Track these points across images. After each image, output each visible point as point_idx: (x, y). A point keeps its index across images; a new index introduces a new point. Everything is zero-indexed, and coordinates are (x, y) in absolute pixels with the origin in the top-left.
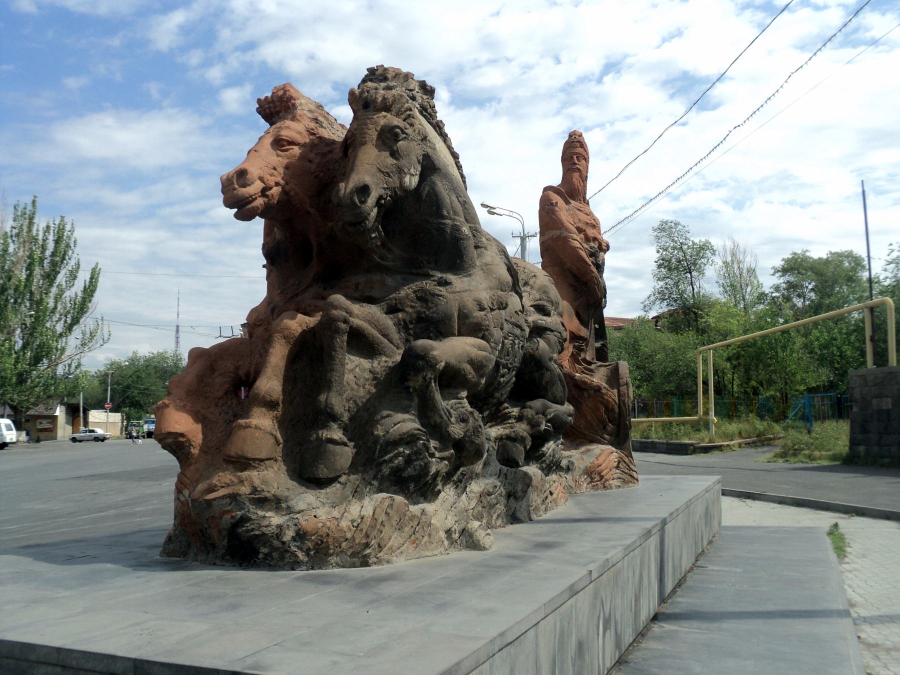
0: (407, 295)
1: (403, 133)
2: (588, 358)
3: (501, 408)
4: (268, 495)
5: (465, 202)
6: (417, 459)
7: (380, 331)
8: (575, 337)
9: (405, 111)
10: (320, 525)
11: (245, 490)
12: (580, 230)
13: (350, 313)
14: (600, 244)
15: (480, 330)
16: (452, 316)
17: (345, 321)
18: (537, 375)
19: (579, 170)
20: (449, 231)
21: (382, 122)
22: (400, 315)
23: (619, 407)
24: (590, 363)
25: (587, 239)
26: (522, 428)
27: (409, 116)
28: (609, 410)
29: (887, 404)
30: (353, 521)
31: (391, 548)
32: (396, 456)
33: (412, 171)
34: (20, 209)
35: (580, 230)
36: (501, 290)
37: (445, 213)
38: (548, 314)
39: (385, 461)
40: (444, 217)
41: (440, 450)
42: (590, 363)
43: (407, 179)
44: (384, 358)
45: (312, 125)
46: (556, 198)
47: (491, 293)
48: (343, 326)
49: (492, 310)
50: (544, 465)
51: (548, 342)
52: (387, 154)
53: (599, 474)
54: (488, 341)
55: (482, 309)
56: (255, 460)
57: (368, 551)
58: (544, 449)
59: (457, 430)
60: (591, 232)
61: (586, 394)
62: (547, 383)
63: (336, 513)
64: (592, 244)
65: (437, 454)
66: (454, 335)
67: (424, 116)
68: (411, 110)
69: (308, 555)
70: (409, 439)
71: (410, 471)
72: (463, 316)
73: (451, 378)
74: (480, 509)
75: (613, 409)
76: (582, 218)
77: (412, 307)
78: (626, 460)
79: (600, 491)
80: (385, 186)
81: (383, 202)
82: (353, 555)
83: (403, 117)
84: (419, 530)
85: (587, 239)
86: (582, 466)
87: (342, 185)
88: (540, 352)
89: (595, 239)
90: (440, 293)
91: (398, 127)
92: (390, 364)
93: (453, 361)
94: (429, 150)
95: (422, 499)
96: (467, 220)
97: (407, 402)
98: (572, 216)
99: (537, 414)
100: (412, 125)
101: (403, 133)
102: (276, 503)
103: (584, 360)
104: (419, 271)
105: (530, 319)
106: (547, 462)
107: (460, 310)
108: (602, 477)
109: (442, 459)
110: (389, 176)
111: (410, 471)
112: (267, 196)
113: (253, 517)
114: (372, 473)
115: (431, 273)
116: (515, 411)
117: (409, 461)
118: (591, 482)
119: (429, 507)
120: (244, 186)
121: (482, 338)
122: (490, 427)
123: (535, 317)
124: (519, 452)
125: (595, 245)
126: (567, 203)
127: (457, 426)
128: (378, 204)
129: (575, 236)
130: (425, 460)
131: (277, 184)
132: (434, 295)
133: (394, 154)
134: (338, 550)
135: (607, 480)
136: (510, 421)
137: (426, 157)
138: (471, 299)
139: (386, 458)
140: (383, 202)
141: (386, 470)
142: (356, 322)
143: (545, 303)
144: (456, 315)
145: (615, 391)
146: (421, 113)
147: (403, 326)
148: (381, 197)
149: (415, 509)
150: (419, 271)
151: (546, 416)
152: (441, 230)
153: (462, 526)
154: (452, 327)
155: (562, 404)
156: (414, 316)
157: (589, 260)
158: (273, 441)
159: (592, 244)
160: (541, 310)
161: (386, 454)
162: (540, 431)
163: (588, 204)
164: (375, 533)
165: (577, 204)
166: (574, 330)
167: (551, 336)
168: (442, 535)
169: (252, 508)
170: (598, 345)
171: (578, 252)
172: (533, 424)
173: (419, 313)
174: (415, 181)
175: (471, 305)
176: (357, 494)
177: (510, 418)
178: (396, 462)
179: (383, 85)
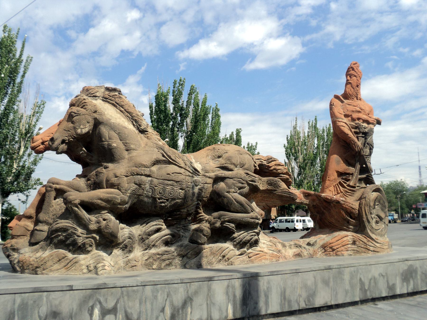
2: (351, 183)
3: (197, 216)
4: (15, 247)
5: (119, 133)
6: (71, 237)
8: (340, 174)
9: (83, 103)
11: (9, 245)
15: (115, 186)
16: (103, 180)
18: (220, 200)
19: (350, 83)
20: (106, 147)
23: (359, 210)
25: (353, 120)
26: (205, 226)
27: (84, 105)
28: (350, 213)
30: (36, 258)
31: (51, 270)
32: (60, 235)
33: (82, 127)
34: (311, 123)
35: (346, 116)
36: (136, 167)
37: (104, 140)
38: (231, 170)
39: (52, 238)
40: (103, 141)
41: (87, 234)
46: (337, 102)
47: (127, 169)
50: (235, 243)
51: (227, 184)
52: (70, 123)
53: (331, 248)
54: (120, 190)
55: (116, 177)
56: (15, 236)
57: (38, 269)
60: (355, 115)
61: (332, 205)
62: (227, 203)
63: (31, 255)
64: (357, 122)
65: (85, 236)
69: (20, 268)
70: (64, 230)
71: (68, 242)
72: (107, 181)
74: (151, 260)
75: (352, 213)
76: (349, 109)
77: (93, 178)
78: (365, 240)
79: (332, 257)
80: (67, 135)
81: (67, 141)
82: (33, 270)
85: (353, 120)
86: (321, 243)
88: (219, 189)
89: (359, 119)
91: (72, 112)
95: (82, 253)
96: (121, 140)
97: (68, 216)
98: (343, 109)
99: (214, 219)
100: (85, 109)
103: (349, 185)
105: (212, 175)
106: (237, 241)
108: (333, 250)
109: (87, 238)
110: (69, 131)
111: (68, 242)
113: (11, 254)
114: (49, 241)
115: (103, 164)
116: (207, 217)
117: (67, 238)
118: (325, 252)
119: (82, 256)
120: (33, 143)
121: (118, 189)
122: (193, 225)
126: (342, 102)
127: (95, 225)
129: (340, 120)
133: (73, 122)
134: (28, 268)
135: (338, 251)
136: (203, 222)
137: (95, 119)
139: (53, 236)
141: (55, 241)
143: (226, 165)
144: (105, 180)
145: (359, 201)
149: (70, 256)
151: (220, 220)
152: (103, 147)
153: (95, 265)
154: (103, 185)
156: (93, 182)
158: (25, 229)
159: (357, 122)
161: (53, 235)
162: (216, 227)
163: (360, 100)
165: (350, 101)
166: (340, 170)
167: (228, 181)
168: (84, 267)
169: (11, 251)
170: (364, 176)
171: (340, 129)
172: (212, 224)
173: (94, 180)
176: (43, 249)
177: (203, 221)
178: (59, 238)
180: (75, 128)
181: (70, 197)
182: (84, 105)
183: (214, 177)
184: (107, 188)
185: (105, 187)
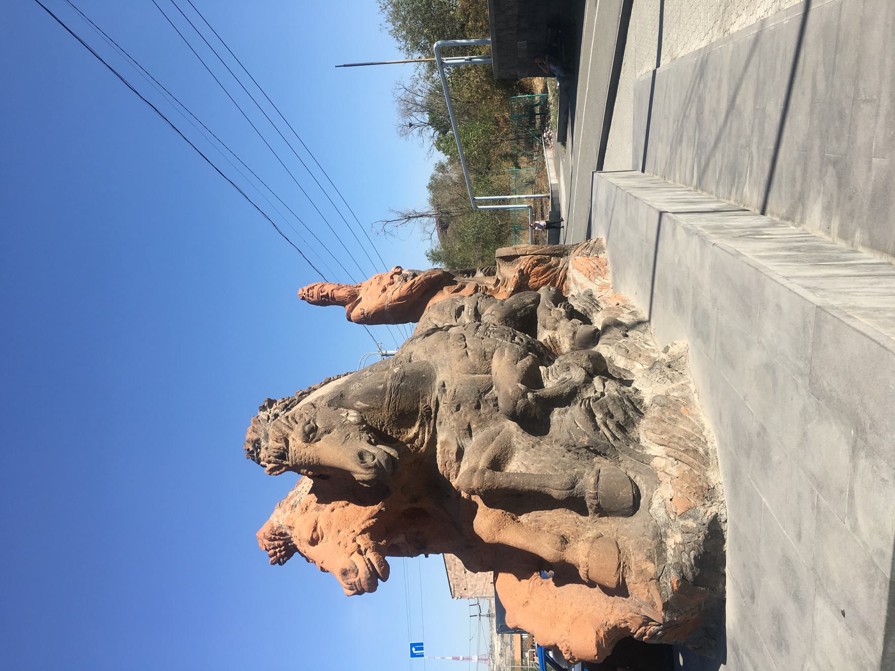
0: (455, 420)
1: (309, 423)
2: (494, 282)
7: (489, 444)
10: (679, 495)
12: (384, 290)
13: (473, 470)
14: (396, 273)
16: (474, 382)
17: (483, 472)
21: (299, 442)
22: (473, 426)
24: (498, 281)
29: (522, 45)
35: (384, 290)
40: (385, 388)
42: (498, 281)
43: (352, 419)
44: (514, 439)
45: (298, 509)
48: (487, 474)
49: (466, 346)
58: (579, 310)
59: (577, 375)
66: (490, 379)
67: (292, 407)
68: (287, 417)
73: (532, 379)
77: (465, 416)
81: (373, 440)
83: (293, 423)
84: (672, 406)
87: (357, 477)
89: (392, 277)
90: (452, 392)
91: (304, 427)
92: (520, 433)
93: (516, 377)
94: (323, 402)
101: (309, 423)
102: (659, 538)
104: (433, 410)
106: (591, 307)
107: (468, 373)
112: (366, 550)
123: (466, 317)
124: (583, 330)
125: (396, 277)
128: (375, 444)
130: (608, 400)
131: (354, 541)
132: (454, 397)
138: (458, 364)
140: (373, 440)
142: (482, 463)
144: (473, 376)
146: (289, 409)
147: (483, 422)
148: (369, 442)
150: (433, 410)
155: (539, 296)
157: (410, 282)
160: (459, 312)
164: (682, 443)
174: (352, 413)
175: (463, 364)
179: (263, 443)
180: (343, 425)
181: (510, 391)
182: (293, 418)
183: (473, 320)
184: (488, 372)
185: (489, 375)
